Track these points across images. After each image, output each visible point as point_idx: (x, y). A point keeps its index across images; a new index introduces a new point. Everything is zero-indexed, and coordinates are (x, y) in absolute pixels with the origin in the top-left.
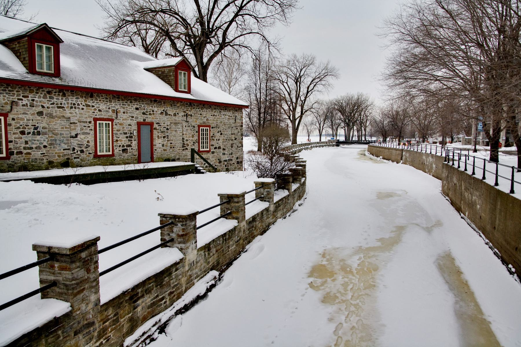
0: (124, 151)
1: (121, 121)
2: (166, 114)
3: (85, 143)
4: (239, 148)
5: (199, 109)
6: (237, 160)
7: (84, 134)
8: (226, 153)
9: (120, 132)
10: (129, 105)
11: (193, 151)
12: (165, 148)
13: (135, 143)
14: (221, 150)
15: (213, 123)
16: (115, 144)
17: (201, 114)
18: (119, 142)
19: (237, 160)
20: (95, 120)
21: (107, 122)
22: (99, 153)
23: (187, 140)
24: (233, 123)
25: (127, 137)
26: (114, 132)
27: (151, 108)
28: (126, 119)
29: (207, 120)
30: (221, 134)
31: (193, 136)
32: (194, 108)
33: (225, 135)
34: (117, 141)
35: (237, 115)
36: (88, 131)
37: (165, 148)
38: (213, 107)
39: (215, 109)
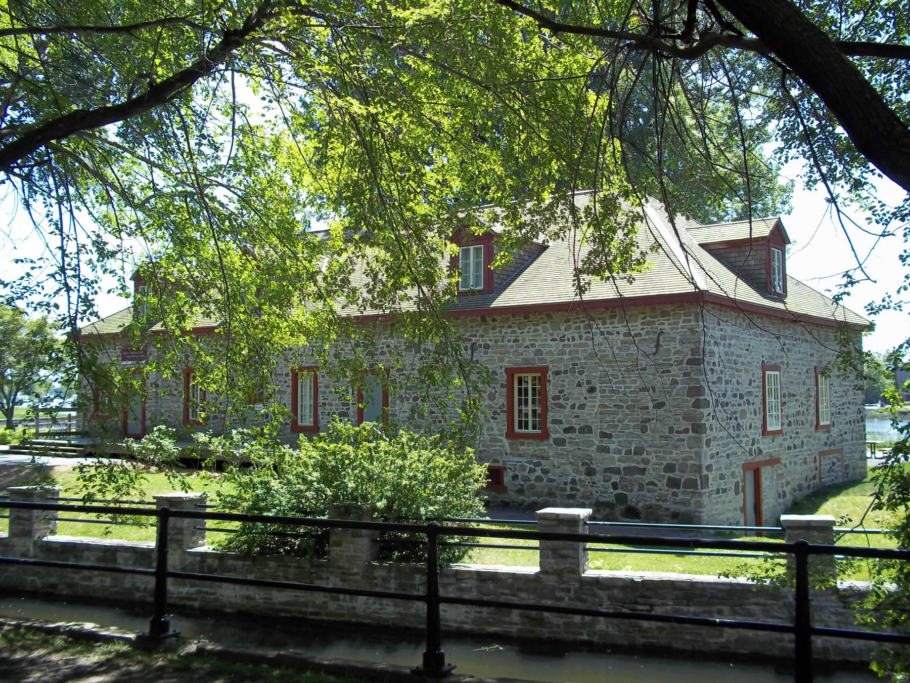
4: (675, 436)
5: (509, 327)
6: (671, 475)
8: (612, 447)
14: (595, 439)
17: (516, 341)
18: (327, 407)
19: (671, 475)
26: (320, 390)
27: (384, 340)
29: (539, 352)
30: (592, 390)
32: (493, 328)
33: (613, 391)
34: (324, 404)
35: (666, 327)
36: (284, 389)
38: (557, 316)
39: (568, 321)
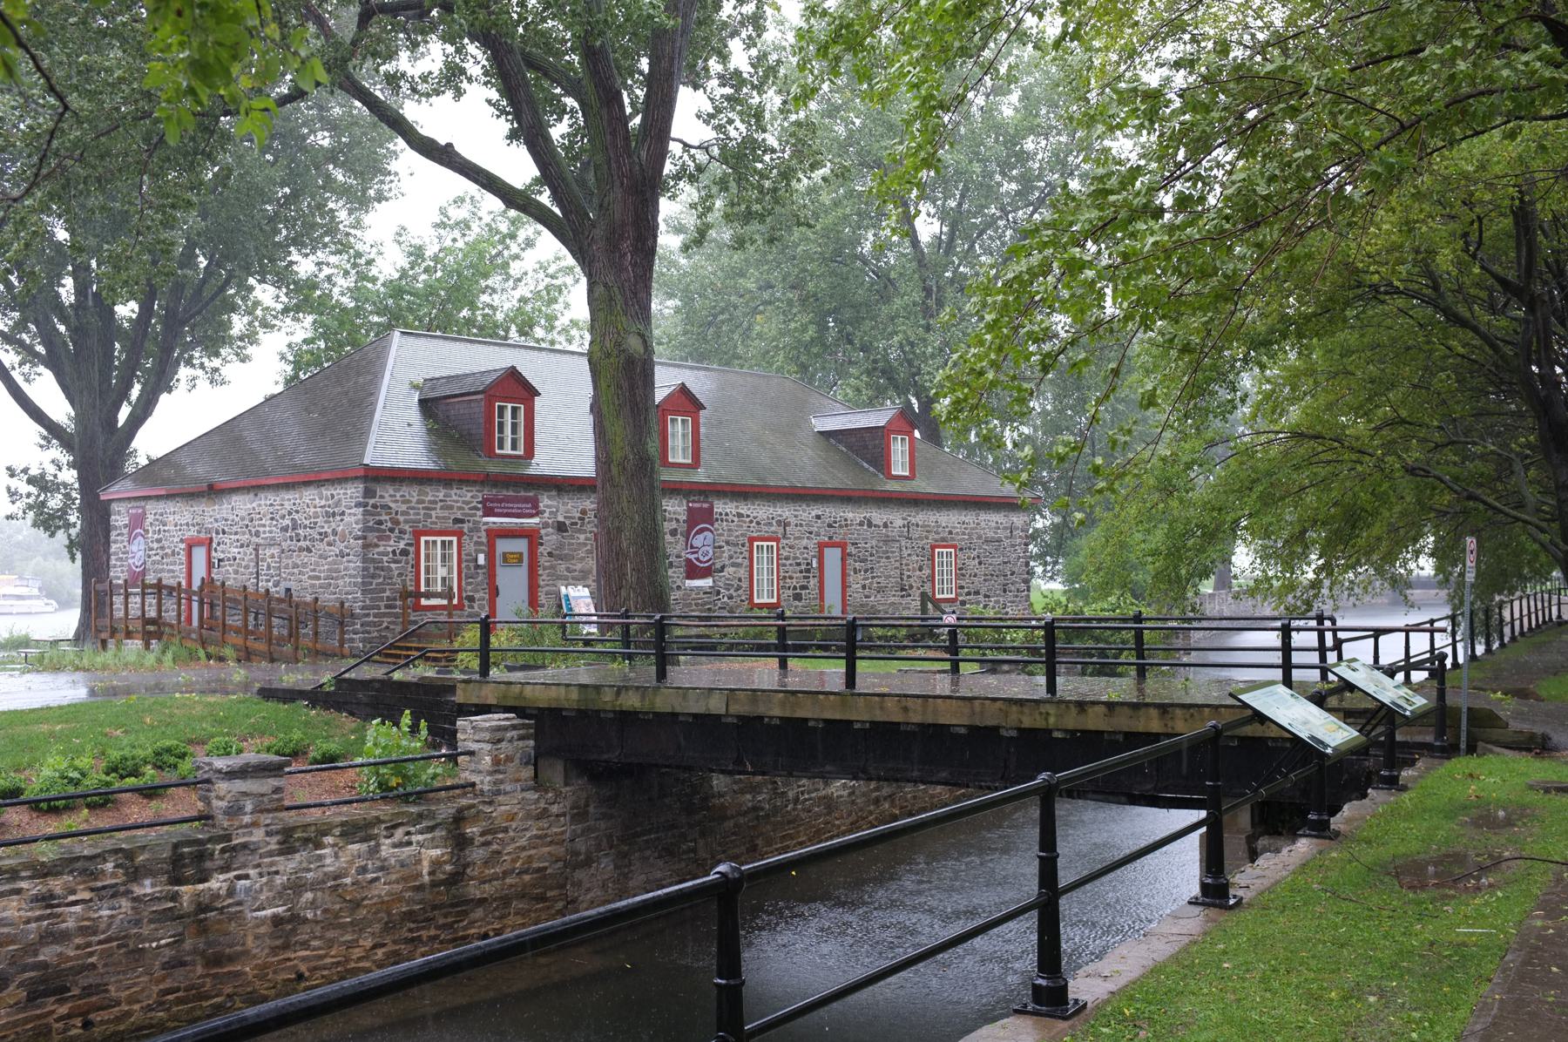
1: (791, 542)
2: (870, 524)
3: (735, 583)
7: (733, 565)
9: (788, 562)
10: (804, 511)
11: (924, 596)
12: (867, 592)
13: (813, 582)
14: (981, 598)
15: (963, 540)
16: (781, 582)
20: (752, 540)
21: (770, 543)
22: (756, 601)
23: (909, 577)
24: (1007, 538)
25: (801, 572)
28: (799, 538)
29: (950, 533)
30: (980, 563)
31: (920, 569)
36: (740, 560)
37: (867, 592)
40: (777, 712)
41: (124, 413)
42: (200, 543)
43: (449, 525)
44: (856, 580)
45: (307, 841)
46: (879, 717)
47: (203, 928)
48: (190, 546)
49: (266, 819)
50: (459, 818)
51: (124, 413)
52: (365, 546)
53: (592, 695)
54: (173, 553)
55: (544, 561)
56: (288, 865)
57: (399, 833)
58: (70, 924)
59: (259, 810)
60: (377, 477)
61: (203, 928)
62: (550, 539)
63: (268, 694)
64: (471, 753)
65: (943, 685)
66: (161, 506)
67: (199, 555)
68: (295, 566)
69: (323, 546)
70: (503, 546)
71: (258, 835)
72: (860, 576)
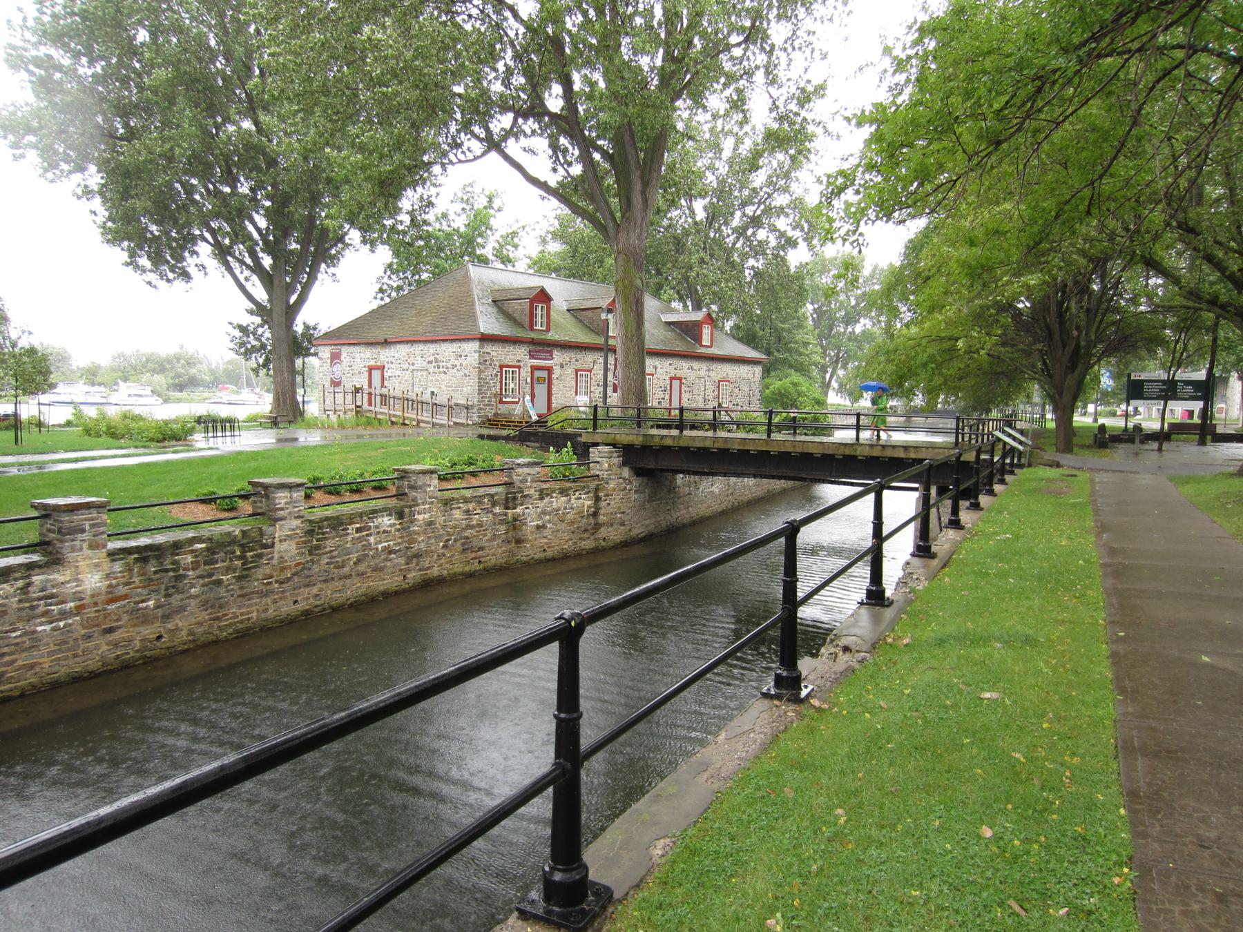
0: (660, 403)
13: (667, 397)
40: (737, 447)
41: (293, 299)
42: (377, 368)
43: (515, 363)
44: (685, 396)
45: (548, 495)
46: (783, 449)
47: (515, 528)
48: (371, 369)
49: (535, 484)
50: (597, 490)
51: (293, 299)
52: (480, 372)
53: (649, 438)
54: (359, 373)
55: (555, 382)
56: (541, 504)
57: (577, 493)
58: (474, 522)
59: (533, 481)
60: (485, 339)
61: (515, 528)
62: (557, 372)
63: (481, 437)
64: (598, 462)
65: (790, 438)
66: (351, 349)
67: (376, 375)
68: (437, 380)
69: (455, 371)
70: (538, 374)
71: (532, 491)
72: (687, 394)
